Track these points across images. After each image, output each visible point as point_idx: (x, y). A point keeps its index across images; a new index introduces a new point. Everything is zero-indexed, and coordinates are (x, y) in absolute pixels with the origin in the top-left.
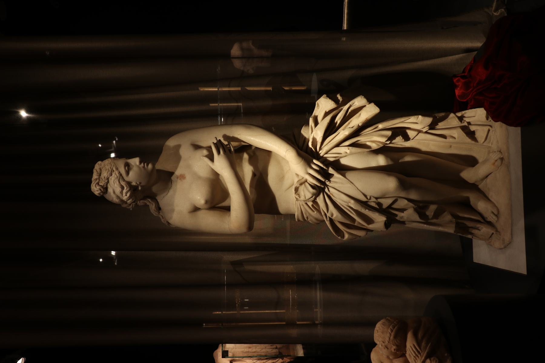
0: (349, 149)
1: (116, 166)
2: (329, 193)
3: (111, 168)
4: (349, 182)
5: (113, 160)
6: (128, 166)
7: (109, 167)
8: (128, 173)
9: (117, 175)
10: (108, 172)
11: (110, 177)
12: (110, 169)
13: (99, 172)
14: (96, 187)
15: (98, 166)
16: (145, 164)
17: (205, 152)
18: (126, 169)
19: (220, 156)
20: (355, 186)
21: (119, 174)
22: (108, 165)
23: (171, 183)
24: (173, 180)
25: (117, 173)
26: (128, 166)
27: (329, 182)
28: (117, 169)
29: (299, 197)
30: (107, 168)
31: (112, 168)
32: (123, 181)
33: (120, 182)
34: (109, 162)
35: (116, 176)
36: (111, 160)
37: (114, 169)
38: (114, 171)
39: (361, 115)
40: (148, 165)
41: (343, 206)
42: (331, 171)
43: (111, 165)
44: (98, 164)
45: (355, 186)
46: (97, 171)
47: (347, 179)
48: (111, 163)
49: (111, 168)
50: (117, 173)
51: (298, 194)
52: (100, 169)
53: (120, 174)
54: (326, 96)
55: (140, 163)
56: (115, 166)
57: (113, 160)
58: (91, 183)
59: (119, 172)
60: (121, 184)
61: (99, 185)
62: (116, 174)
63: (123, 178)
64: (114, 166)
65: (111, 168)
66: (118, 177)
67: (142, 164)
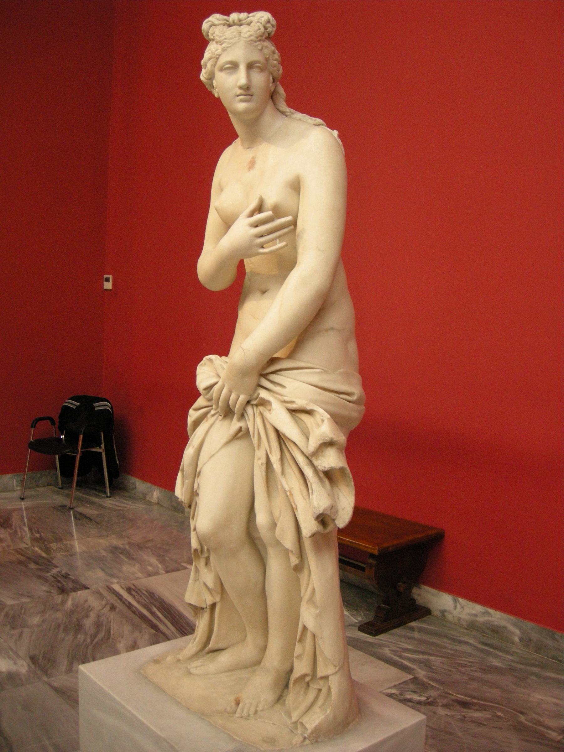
0: (262, 464)
1: (228, 47)
2: (209, 416)
3: (225, 39)
4: (212, 453)
5: (245, 39)
6: (234, 66)
7: (227, 36)
8: (222, 69)
9: (216, 53)
10: (217, 35)
11: (214, 42)
12: (223, 38)
13: (244, 21)
14: (207, 22)
15: (259, 17)
16: (242, 97)
17: (270, 201)
18: (225, 65)
19: (248, 228)
20: (208, 460)
21: (217, 55)
22: (233, 34)
23: (248, 147)
24: (252, 149)
25: (219, 51)
26: (234, 66)
27: (220, 419)
28: (224, 50)
29: (201, 365)
30: (225, 34)
31: (224, 42)
32: (212, 65)
33: (210, 59)
34: (242, 35)
35: (214, 50)
36: (247, 35)
37: (224, 45)
38: (221, 45)
39: (305, 501)
40: (242, 101)
41: (195, 435)
42: (235, 425)
43: (232, 38)
44: (262, 17)
45: (208, 460)
46: (248, 17)
47: (218, 451)
48: (237, 38)
49: (225, 39)
50: (219, 51)
51: (205, 363)
52: (249, 24)
53: (218, 56)
54: (327, 438)
55: (241, 88)
56: (230, 45)
57: (245, 39)
58: (227, 13)
59: (220, 55)
60: (207, 62)
61: (211, 26)
62: (217, 50)
63: (216, 62)
64: (228, 44)
65: (225, 40)
66: (214, 55)
67: (239, 92)
